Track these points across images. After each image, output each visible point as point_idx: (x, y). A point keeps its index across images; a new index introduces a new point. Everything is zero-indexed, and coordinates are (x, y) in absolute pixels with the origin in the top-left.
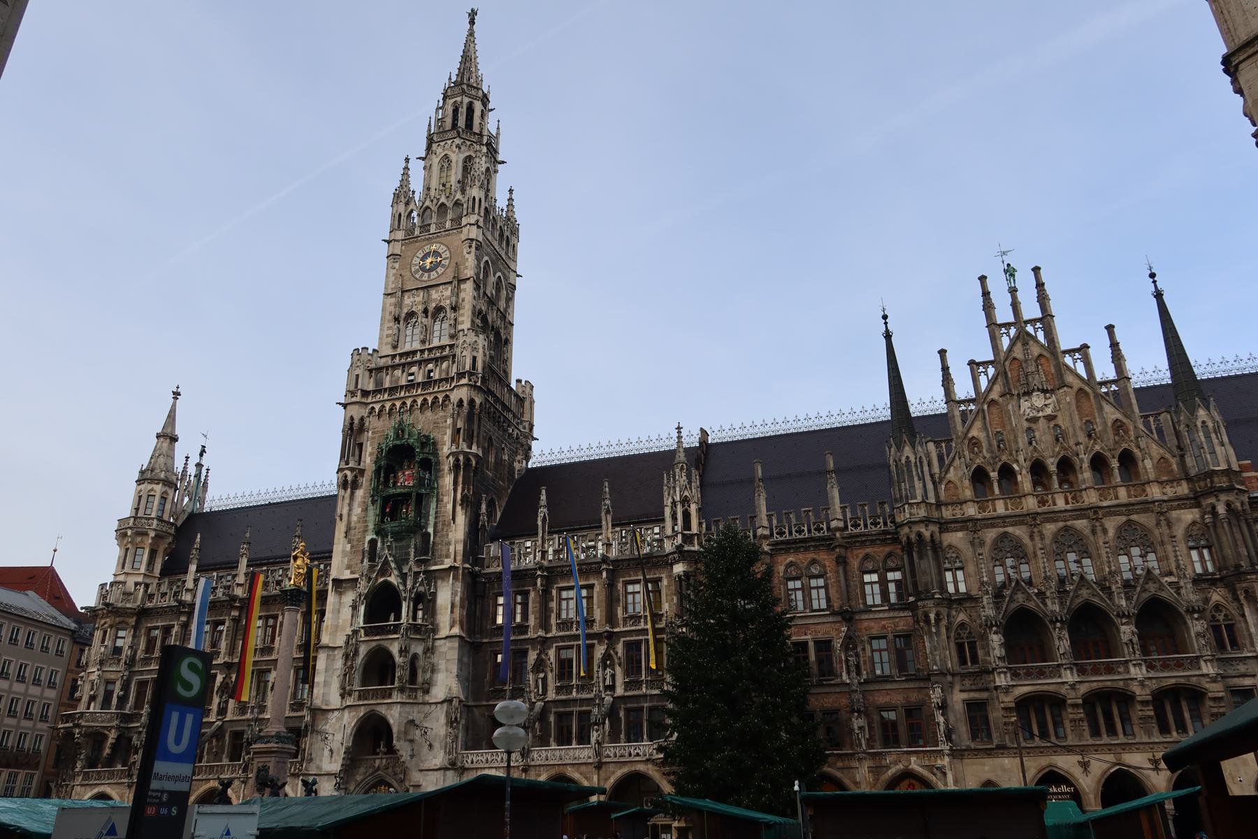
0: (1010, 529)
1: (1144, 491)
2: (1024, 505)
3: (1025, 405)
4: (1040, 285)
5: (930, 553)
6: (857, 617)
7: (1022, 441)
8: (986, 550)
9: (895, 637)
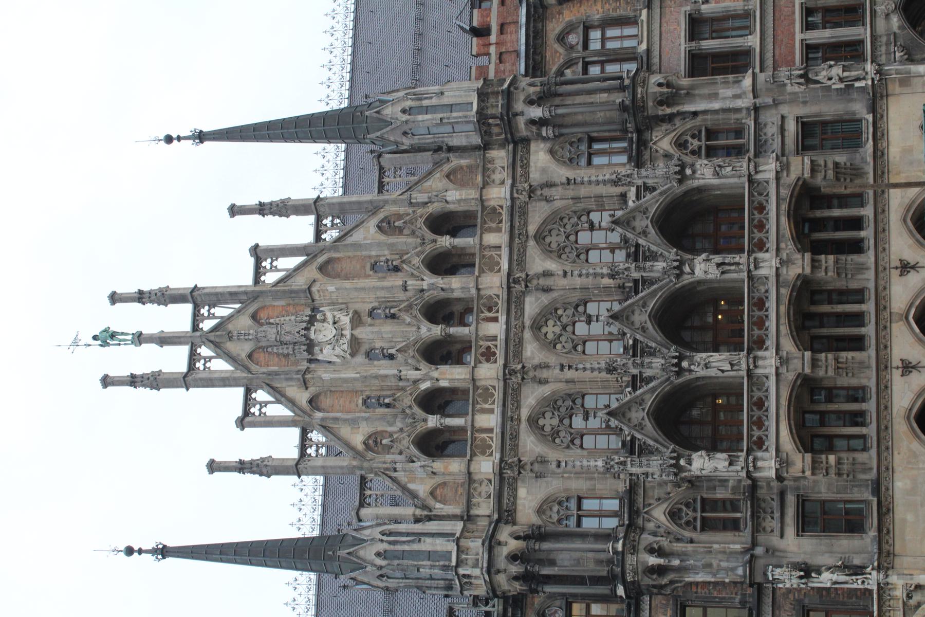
0: (525, 413)
1: (494, 209)
2: (488, 383)
3: (327, 353)
4: (141, 297)
5: (546, 546)
7: (385, 369)
8: (553, 455)
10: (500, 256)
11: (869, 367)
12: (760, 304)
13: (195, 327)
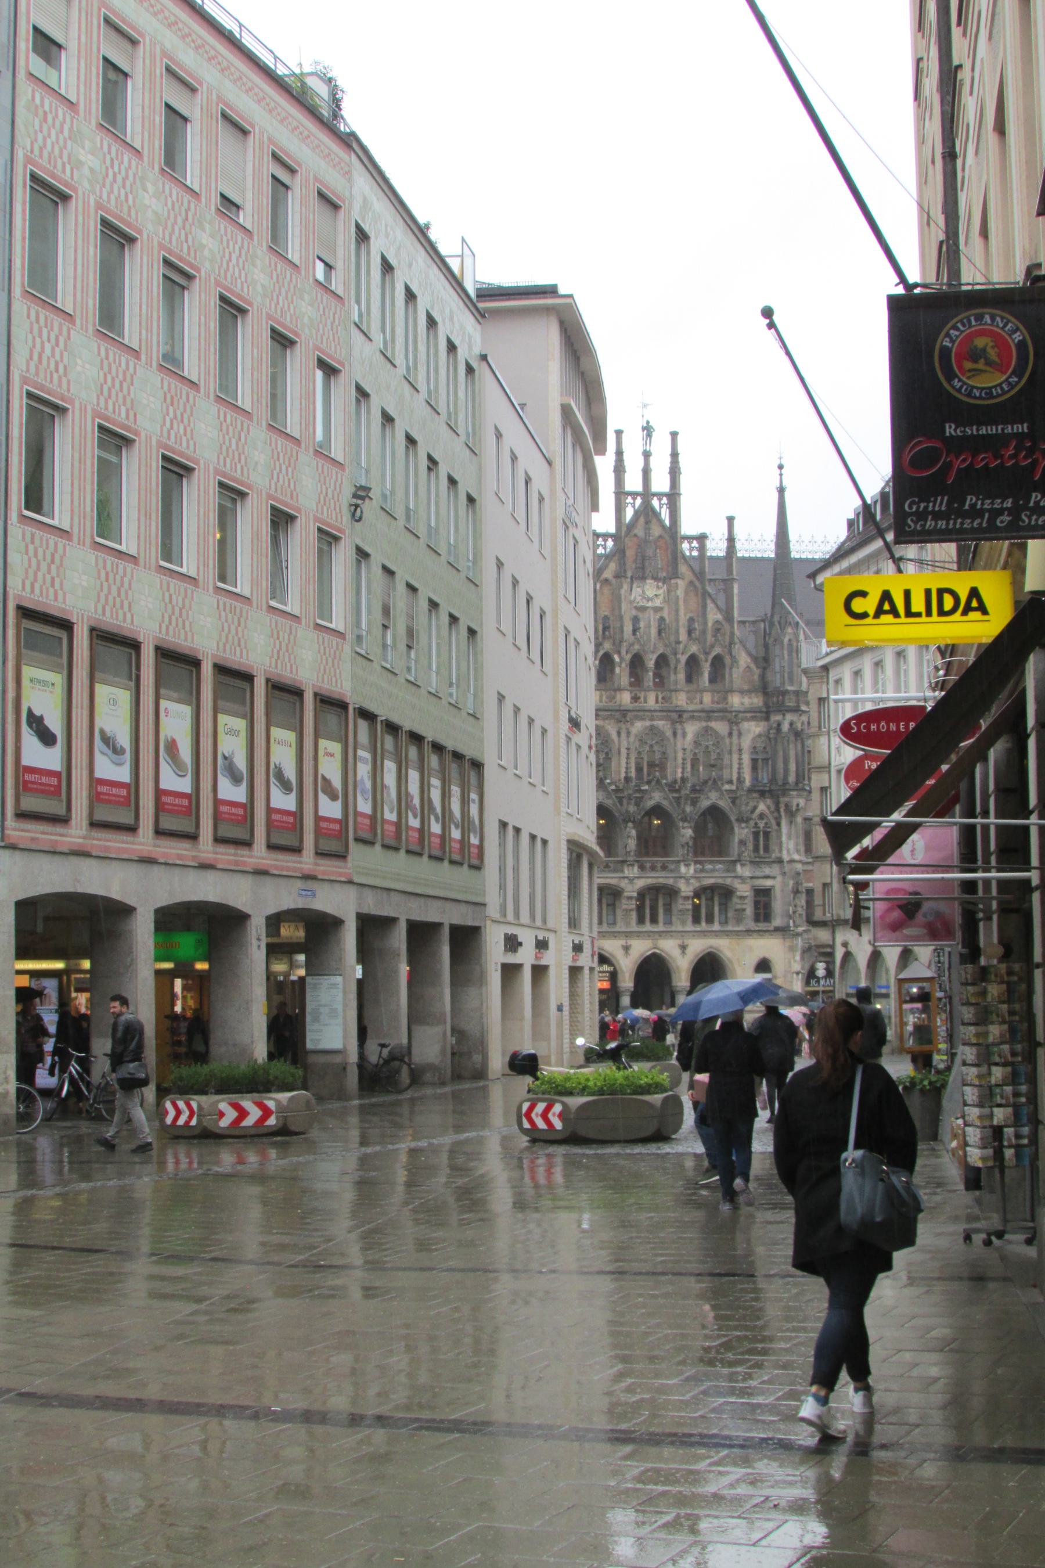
1: (725, 699)
7: (628, 628)
12: (664, 868)
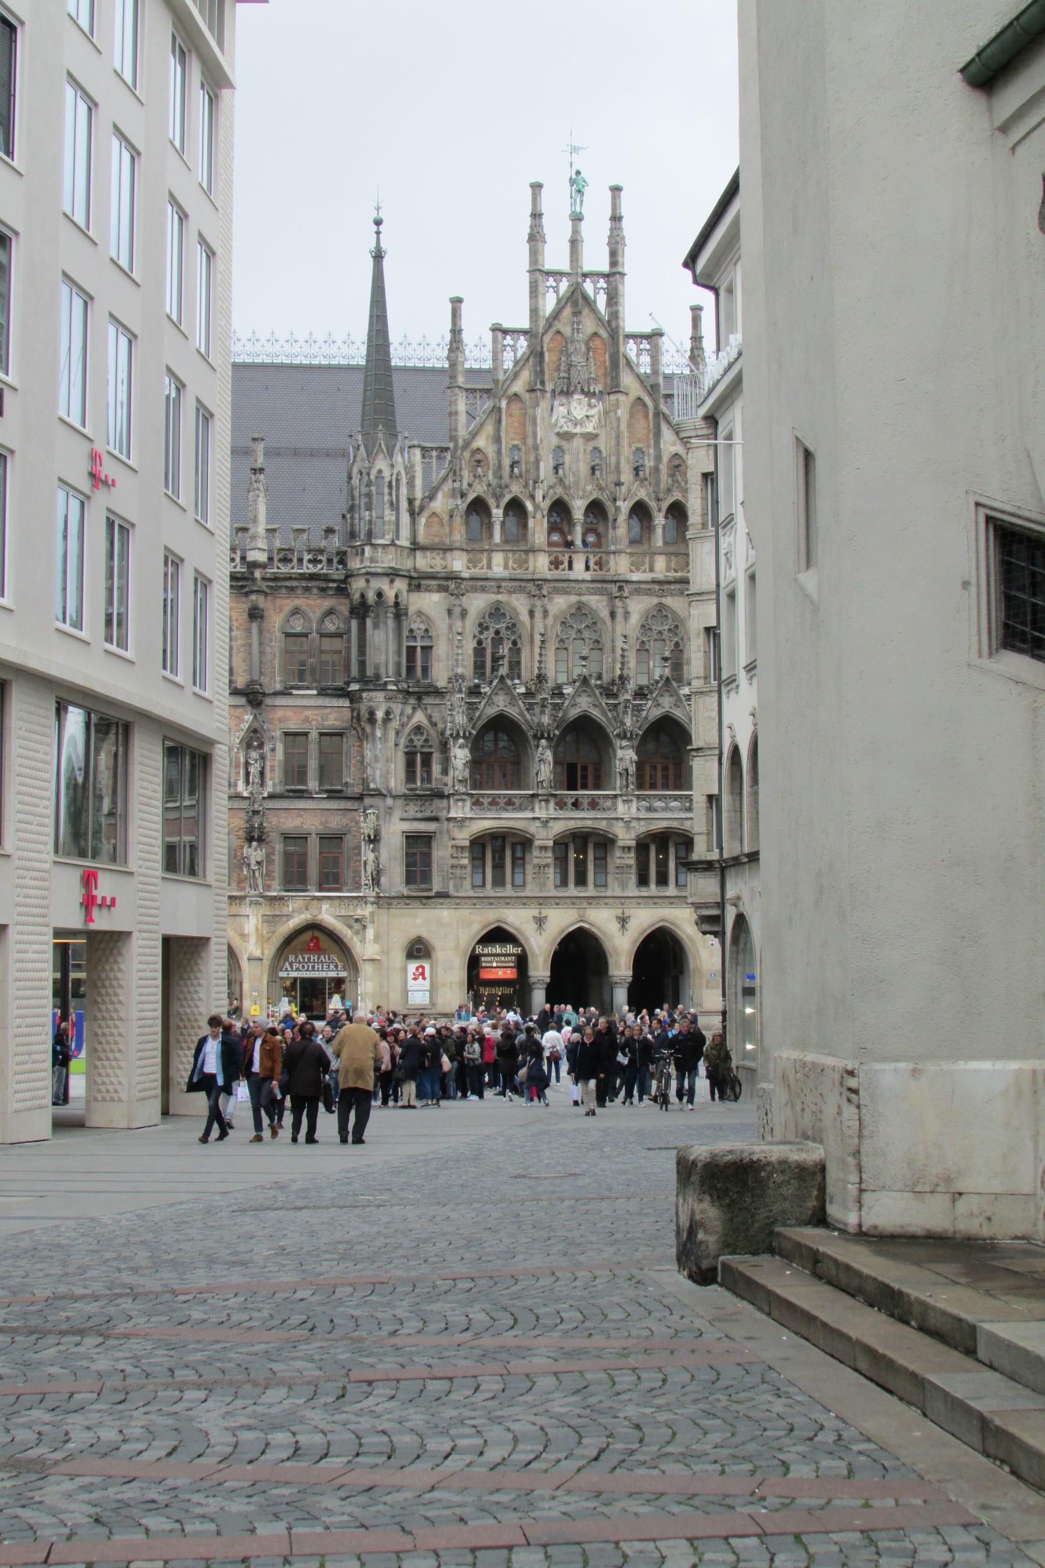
5: (391, 623)
6: (268, 701)
9: (321, 734)
10: (644, 571)
11: (541, 890)
12: (594, 805)
13: (585, 275)
